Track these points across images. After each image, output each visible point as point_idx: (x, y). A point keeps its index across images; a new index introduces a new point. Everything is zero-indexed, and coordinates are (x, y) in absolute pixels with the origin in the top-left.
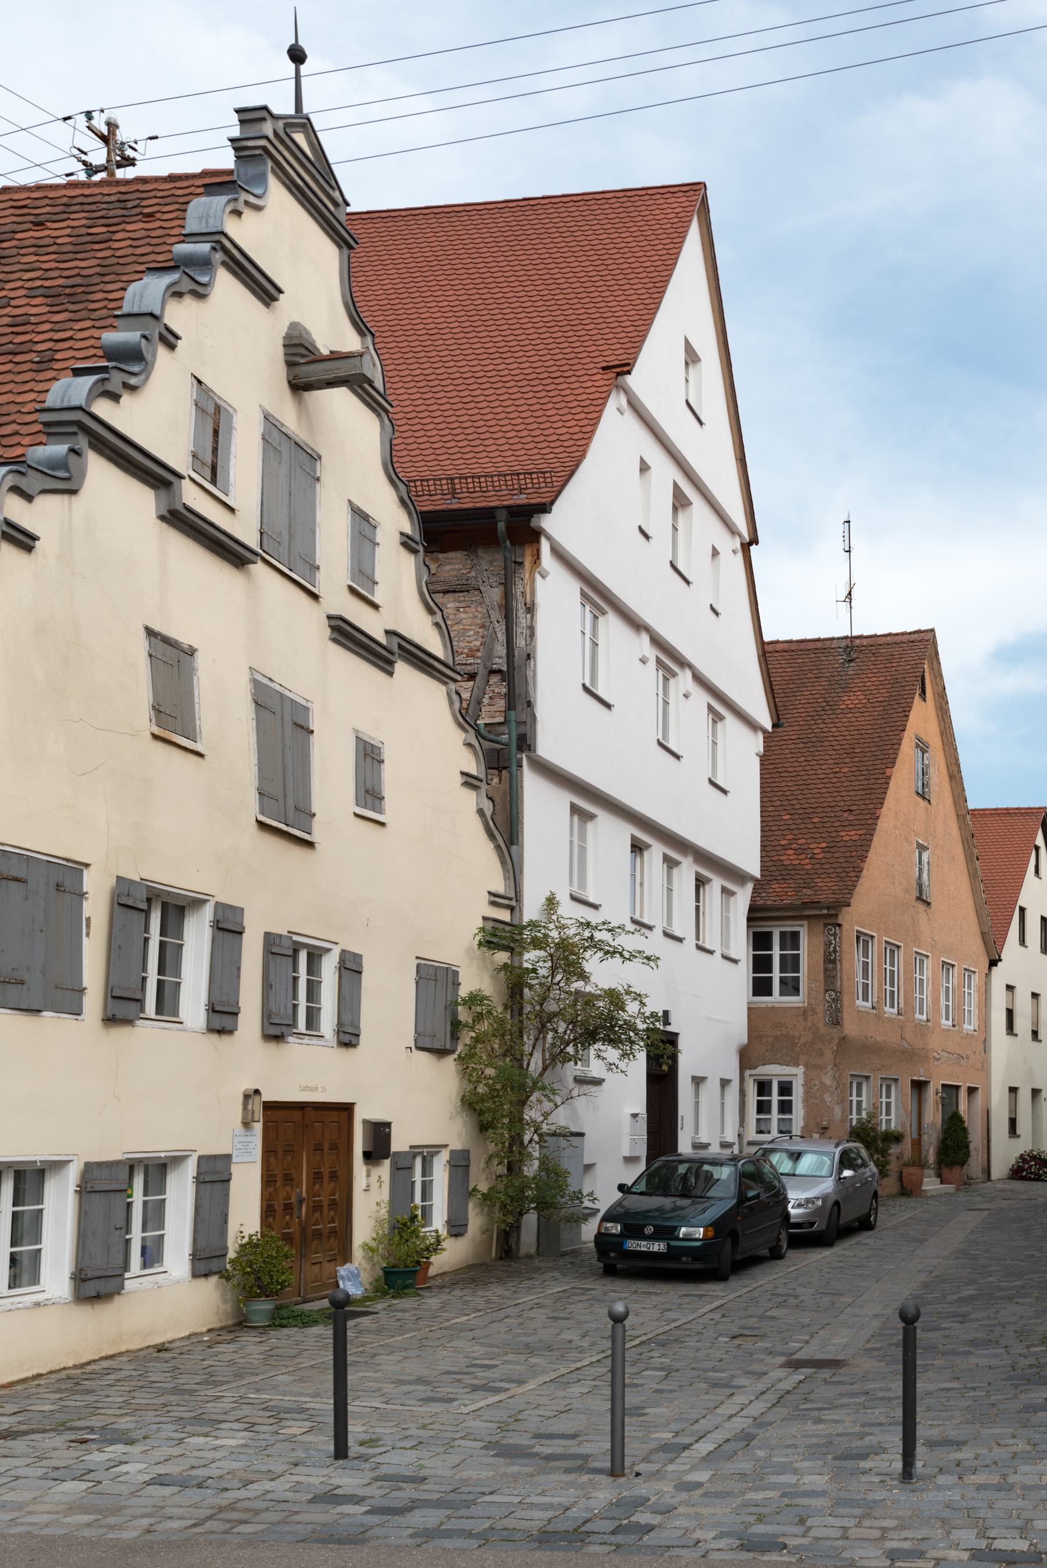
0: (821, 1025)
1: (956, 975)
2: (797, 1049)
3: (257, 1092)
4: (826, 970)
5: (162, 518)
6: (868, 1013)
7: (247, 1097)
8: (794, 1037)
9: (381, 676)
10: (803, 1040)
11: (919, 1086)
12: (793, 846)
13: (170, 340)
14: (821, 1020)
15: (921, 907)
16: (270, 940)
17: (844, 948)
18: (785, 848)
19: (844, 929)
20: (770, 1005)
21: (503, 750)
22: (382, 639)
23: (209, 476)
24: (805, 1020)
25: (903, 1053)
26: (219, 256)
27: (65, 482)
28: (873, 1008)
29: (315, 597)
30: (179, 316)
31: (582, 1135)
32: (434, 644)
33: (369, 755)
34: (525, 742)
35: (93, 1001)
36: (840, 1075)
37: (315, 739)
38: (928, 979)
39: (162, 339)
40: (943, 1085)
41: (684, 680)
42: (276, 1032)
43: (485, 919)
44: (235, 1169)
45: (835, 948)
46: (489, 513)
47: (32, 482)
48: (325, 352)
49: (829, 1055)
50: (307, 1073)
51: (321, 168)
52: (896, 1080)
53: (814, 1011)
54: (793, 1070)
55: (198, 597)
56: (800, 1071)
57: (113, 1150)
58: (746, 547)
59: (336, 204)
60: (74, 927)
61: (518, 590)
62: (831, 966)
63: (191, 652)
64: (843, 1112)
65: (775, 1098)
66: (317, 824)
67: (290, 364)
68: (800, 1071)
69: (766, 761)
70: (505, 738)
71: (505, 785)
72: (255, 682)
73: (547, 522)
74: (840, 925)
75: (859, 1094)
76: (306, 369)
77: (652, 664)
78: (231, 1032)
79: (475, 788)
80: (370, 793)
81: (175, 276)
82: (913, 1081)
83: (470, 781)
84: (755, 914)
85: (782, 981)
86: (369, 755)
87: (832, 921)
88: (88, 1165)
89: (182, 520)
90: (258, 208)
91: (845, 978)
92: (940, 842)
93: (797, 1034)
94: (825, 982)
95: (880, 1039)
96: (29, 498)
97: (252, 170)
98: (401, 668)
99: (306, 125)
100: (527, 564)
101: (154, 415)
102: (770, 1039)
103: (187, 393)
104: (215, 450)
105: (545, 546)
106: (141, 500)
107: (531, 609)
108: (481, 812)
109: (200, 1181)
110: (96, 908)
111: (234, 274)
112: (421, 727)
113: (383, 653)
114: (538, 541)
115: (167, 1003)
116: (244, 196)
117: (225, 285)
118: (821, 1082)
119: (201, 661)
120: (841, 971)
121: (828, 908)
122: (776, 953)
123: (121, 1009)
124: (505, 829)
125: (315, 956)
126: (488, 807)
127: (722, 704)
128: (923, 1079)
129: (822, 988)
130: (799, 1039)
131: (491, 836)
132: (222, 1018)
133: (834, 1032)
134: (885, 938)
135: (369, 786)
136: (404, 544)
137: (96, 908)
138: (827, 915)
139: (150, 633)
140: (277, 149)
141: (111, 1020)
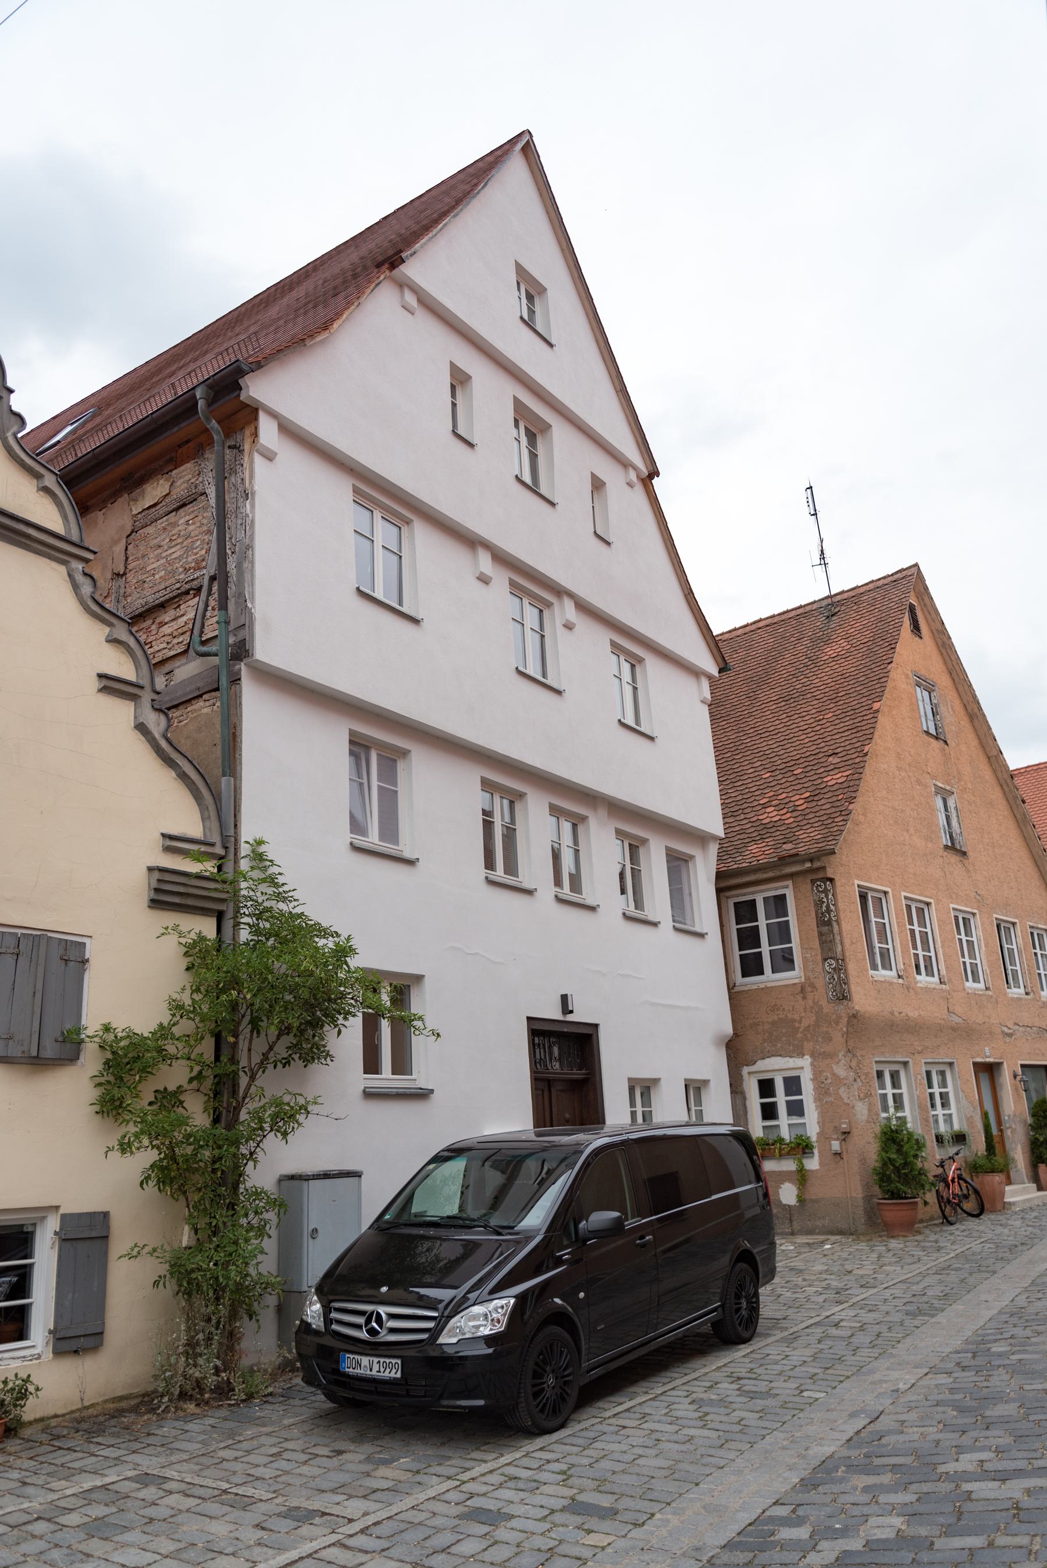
0: (823, 1002)
1: (1019, 934)
2: (799, 1035)
4: (821, 934)
6: (891, 983)
8: (793, 1021)
10: (805, 1023)
11: (988, 1071)
12: (773, 803)
14: (822, 995)
15: (954, 858)
17: (841, 905)
18: (765, 806)
19: (838, 883)
20: (762, 986)
24: (804, 998)
25: (953, 1029)
28: (899, 977)
36: (859, 1063)
38: (978, 940)
40: (1022, 1066)
45: (828, 906)
49: (838, 1038)
52: (951, 1064)
53: (813, 986)
54: (797, 1062)
56: (806, 1062)
62: (825, 929)
64: (870, 1110)
65: (781, 1098)
68: (806, 1062)
74: (831, 880)
75: (896, 1084)
82: (975, 1064)
84: (726, 883)
87: (821, 875)
91: (847, 942)
92: (969, 786)
93: (797, 1017)
94: (822, 949)
95: (913, 1014)
102: (767, 1027)
118: (834, 1074)
120: (840, 934)
121: (811, 861)
128: (991, 1060)
129: (819, 958)
130: (800, 1022)
133: (841, 1009)
134: (903, 894)
138: (814, 869)
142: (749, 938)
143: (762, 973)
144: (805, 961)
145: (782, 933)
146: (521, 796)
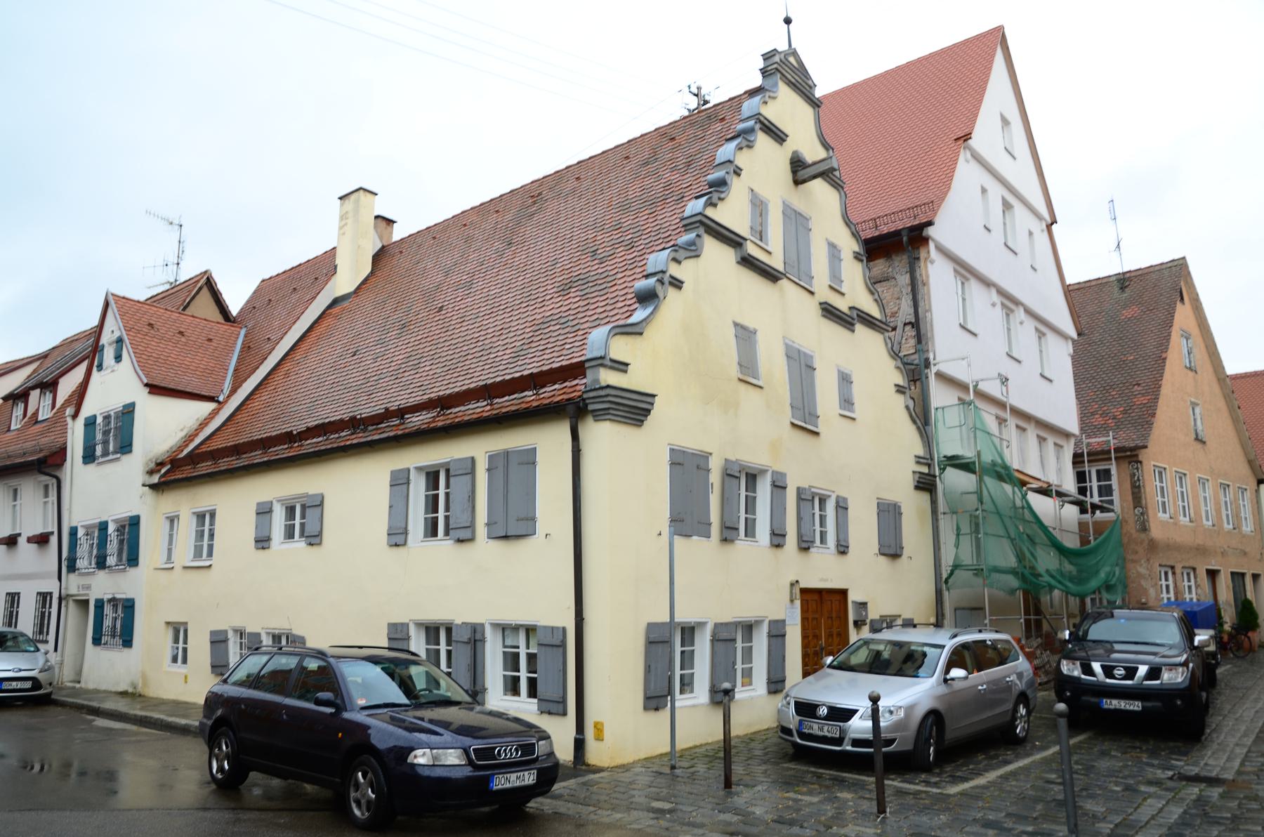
29: (812, 293)
32: (875, 312)
33: (845, 380)
41: (1020, 314)
58: (1049, 227)
72: (786, 345)
77: (999, 306)
79: (903, 393)
80: (847, 402)
83: (900, 390)
86: (845, 380)
89: (748, 262)
98: (859, 327)
105: (932, 245)
108: (907, 407)
112: (870, 360)
119: (760, 337)
124: (922, 417)
131: (914, 422)
139: (736, 324)
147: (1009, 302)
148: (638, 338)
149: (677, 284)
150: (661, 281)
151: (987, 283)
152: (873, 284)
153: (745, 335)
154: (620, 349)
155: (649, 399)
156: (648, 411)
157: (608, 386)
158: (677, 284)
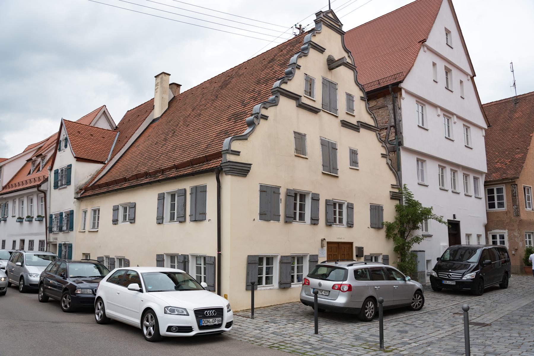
3: (324, 239)
5: (297, 106)
7: (322, 240)
9: (357, 133)
13: (299, 67)
16: (328, 203)
21: (393, 146)
22: (356, 124)
23: (309, 94)
26: (310, 46)
27: (274, 103)
29: (337, 117)
30: (300, 62)
31: (424, 251)
32: (372, 123)
33: (353, 153)
34: (400, 144)
35: (282, 218)
37: (338, 151)
39: (297, 67)
41: (455, 119)
42: (329, 224)
43: (390, 192)
44: (319, 258)
46: (387, 87)
47: (267, 105)
48: (336, 59)
50: (339, 234)
51: (336, 20)
54: (504, 231)
55: (307, 123)
56: (506, 231)
57: (288, 253)
59: (340, 26)
60: (278, 201)
61: (396, 104)
63: (305, 135)
66: (339, 172)
67: (328, 65)
68: (506, 231)
69: (486, 138)
70: (395, 143)
71: (396, 156)
72: (321, 139)
73: (402, 85)
75: (530, 238)
76: (332, 64)
77: (442, 116)
78: (317, 224)
79: (386, 157)
80: (354, 162)
81: (299, 53)
83: (383, 156)
85: (498, 203)
86: (353, 153)
88: (281, 256)
89: (302, 106)
90: (320, 33)
96: (267, 109)
97: (319, 25)
98: (362, 130)
99: (331, 11)
100: (399, 97)
101: (296, 85)
103: (303, 77)
104: (310, 89)
105: (403, 91)
106: (292, 104)
107: (400, 109)
108: (387, 164)
109: (310, 261)
110: (282, 196)
111: (314, 49)
113: (355, 128)
114: (401, 91)
115: (302, 217)
116: (316, 31)
117: (312, 53)
119: (307, 137)
122: (496, 195)
123: (289, 219)
124: (396, 168)
125: (341, 206)
126: (389, 162)
127: (468, 124)
132: (315, 221)
135: (354, 160)
136: (361, 99)
137: (282, 196)
139: (295, 132)
140: (328, 20)
141: (286, 222)
142: (491, 199)
143: (494, 207)
144: (508, 205)
145: (500, 198)
146: (445, 167)
147: (448, 114)
148: (246, 142)
149: (265, 118)
150: (257, 117)
151: (435, 106)
152: (370, 111)
153: (300, 138)
154: (236, 146)
155: (248, 166)
156: (249, 171)
157: (229, 162)
158: (265, 118)
